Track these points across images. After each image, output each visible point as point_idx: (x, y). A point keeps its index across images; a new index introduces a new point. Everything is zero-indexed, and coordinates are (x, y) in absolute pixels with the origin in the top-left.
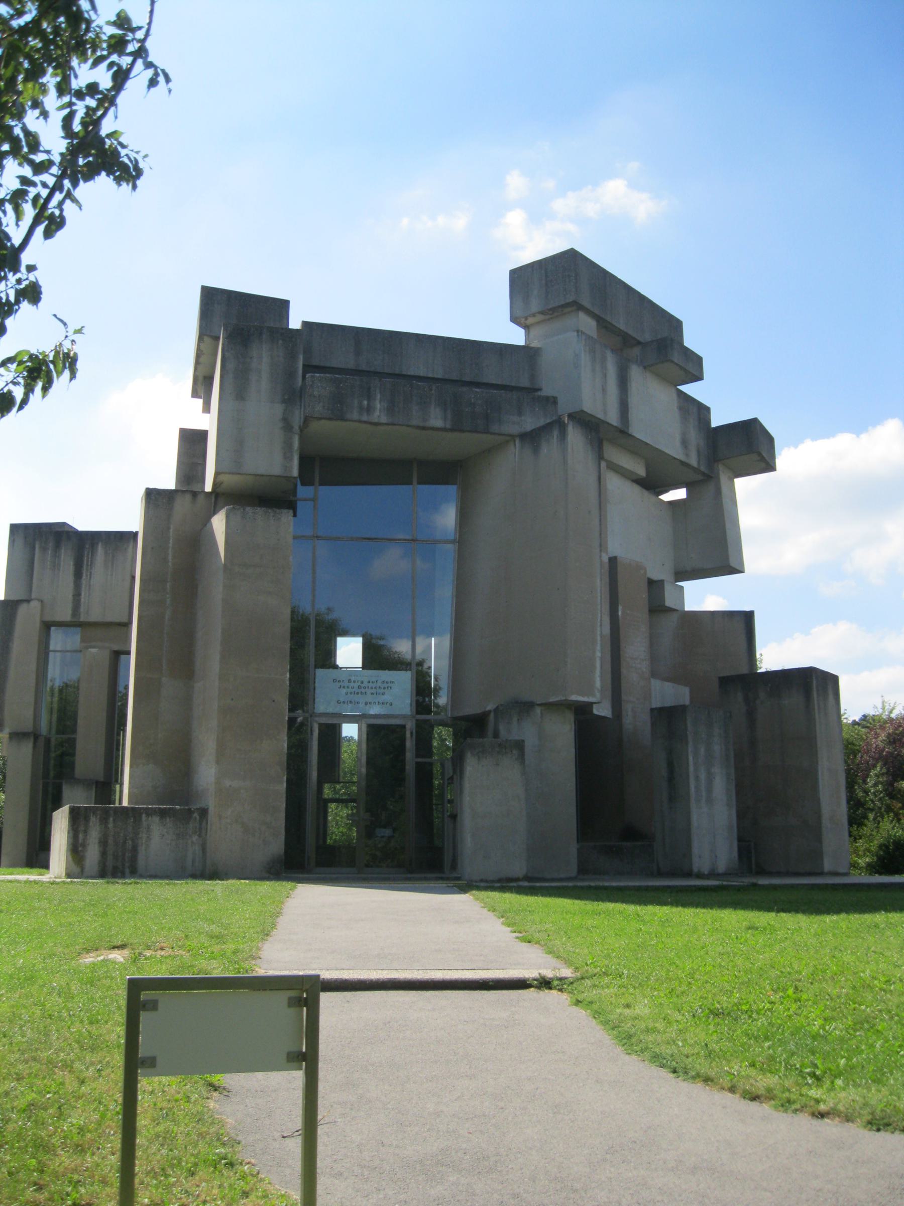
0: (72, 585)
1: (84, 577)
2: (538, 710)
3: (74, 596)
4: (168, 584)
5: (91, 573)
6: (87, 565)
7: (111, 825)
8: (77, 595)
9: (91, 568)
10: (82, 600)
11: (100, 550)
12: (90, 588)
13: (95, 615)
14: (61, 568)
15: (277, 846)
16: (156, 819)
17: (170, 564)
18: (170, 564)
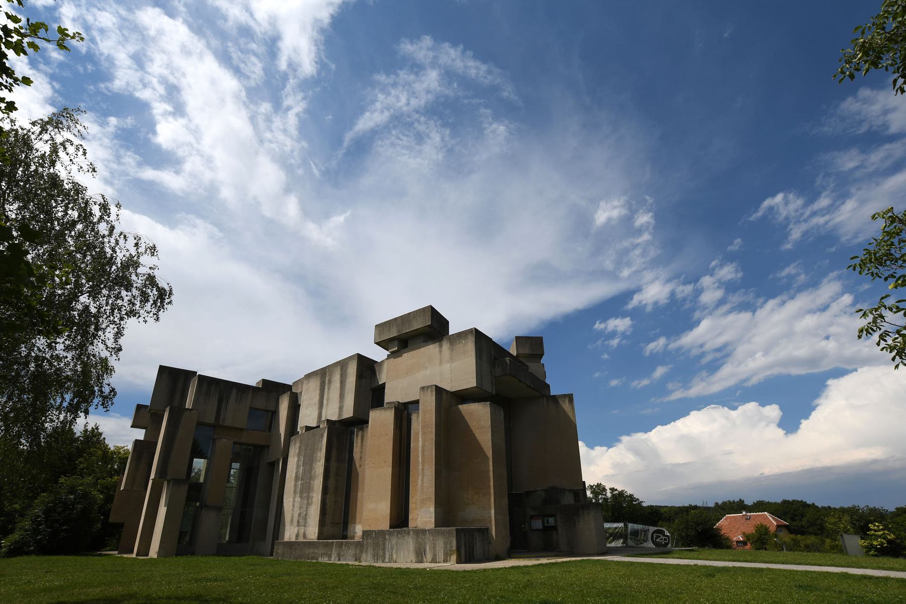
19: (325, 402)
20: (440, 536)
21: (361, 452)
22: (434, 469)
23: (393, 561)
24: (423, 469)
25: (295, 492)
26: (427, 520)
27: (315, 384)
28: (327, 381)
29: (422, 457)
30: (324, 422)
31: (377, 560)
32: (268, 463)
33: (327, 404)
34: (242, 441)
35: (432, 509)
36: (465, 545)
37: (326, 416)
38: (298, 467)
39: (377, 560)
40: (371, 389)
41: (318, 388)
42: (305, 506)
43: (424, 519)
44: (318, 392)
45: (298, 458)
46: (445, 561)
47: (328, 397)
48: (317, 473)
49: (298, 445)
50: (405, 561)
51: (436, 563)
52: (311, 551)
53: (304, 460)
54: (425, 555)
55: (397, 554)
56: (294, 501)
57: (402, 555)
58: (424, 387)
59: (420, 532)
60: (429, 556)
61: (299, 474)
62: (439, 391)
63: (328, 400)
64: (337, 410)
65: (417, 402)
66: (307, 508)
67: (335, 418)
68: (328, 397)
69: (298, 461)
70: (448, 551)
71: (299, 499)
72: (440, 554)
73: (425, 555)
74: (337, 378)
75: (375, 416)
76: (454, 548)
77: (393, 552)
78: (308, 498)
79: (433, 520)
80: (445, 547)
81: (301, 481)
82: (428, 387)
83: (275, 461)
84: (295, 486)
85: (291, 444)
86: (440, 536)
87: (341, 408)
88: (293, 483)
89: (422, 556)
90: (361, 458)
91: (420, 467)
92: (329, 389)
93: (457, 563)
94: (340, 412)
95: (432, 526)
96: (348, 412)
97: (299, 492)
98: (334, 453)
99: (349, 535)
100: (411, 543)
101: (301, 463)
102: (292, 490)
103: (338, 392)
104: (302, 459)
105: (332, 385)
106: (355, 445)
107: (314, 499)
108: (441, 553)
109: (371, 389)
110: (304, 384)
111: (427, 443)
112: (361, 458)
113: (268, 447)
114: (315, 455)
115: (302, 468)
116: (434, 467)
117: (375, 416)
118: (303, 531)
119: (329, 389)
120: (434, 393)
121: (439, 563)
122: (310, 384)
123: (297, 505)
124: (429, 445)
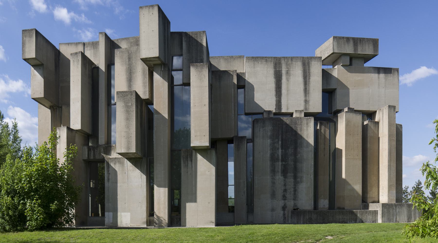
19: (284, 91)
26: (392, 198)
31: (390, 221)
33: (288, 94)
39: (390, 221)
52: (341, 217)
53: (282, 143)
55: (399, 218)
64: (303, 103)
71: (282, 178)
89: (410, 219)
97: (280, 171)
100: (405, 211)
103: (302, 87)
112: (324, 148)
119: (288, 80)
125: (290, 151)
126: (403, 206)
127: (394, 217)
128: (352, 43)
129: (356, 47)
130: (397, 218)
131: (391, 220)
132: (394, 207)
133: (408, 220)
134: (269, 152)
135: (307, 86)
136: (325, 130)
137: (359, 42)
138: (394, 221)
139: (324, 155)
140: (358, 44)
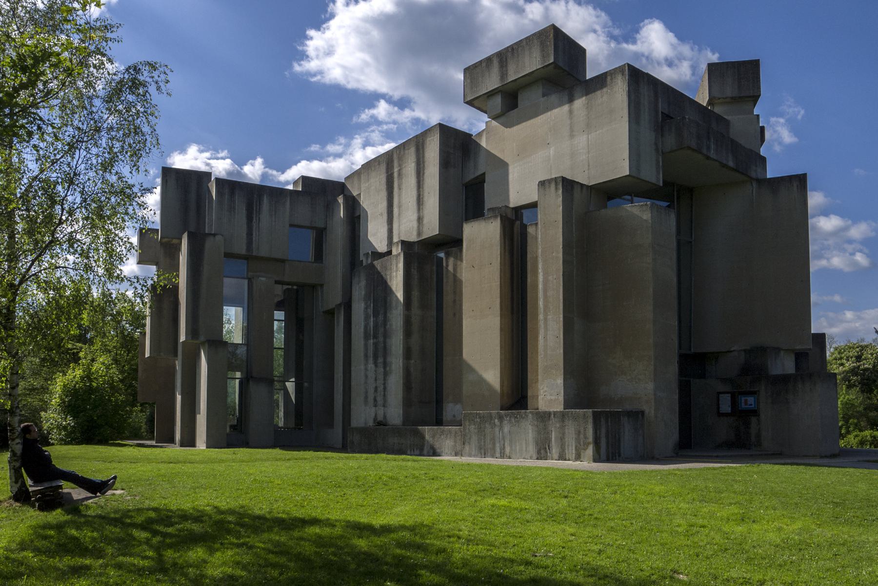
0: (245, 226)
1: (254, 220)
2: (782, 353)
3: (247, 234)
4: (574, 250)
5: (259, 218)
6: (256, 211)
7: (610, 424)
8: (250, 234)
9: (259, 214)
10: (254, 239)
11: (265, 200)
12: (259, 231)
13: (264, 252)
14: (236, 211)
15: (675, 436)
16: (626, 418)
17: (574, 235)
18: (574, 235)
20: (570, 422)
21: (455, 293)
22: (562, 319)
23: (506, 456)
24: (546, 319)
25: (366, 356)
26: (553, 398)
27: (378, 180)
28: (396, 175)
29: (544, 300)
30: (398, 246)
32: (323, 312)
33: (399, 214)
34: (286, 279)
35: (560, 381)
36: (607, 437)
37: (399, 234)
38: (367, 318)
40: (463, 185)
41: (384, 187)
42: (381, 377)
43: (549, 397)
44: (384, 194)
45: (366, 304)
46: (578, 458)
47: (399, 202)
48: (394, 327)
49: (363, 283)
50: (523, 456)
51: (565, 460)
53: (373, 306)
54: (549, 449)
56: (366, 369)
57: (518, 448)
58: (544, 181)
59: (544, 417)
60: (555, 451)
61: (369, 328)
62: (568, 185)
63: (400, 207)
64: (415, 224)
65: (534, 205)
66: (385, 379)
67: (413, 238)
68: (399, 202)
69: (366, 308)
70: (582, 443)
71: (373, 366)
72: (570, 448)
73: (549, 449)
74: (410, 167)
75: (472, 231)
76: (591, 439)
77: (506, 444)
78: (385, 364)
79: (561, 398)
80: (578, 440)
81: (373, 339)
82: (550, 181)
83: (334, 309)
84: (366, 345)
85: (353, 282)
86: (570, 422)
87: (420, 219)
88: (362, 342)
89: (546, 452)
90: (454, 301)
91: (541, 317)
92: (400, 189)
93: (595, 461)
94: (419, 227)
95: (560, 408)
96: (432, 227)
98: (415, 294)
99: (444, 419)
100: (530, 431)
101: (370, 311)
102: (362, 354)
103: (414, 193)
104: (372, 305)
105: (404, 180)
106: (445, 280)
107: (393, 367)
108: (572, 446)
109: (463, 185)
110: (362, 181)
111: (550, 278)
112: (454, 301)
113: (322, 286)
114: (389, 298)
115: (372, 319)
116: (562, 316)
117: (472, 231)
118: (383, 412)
119: (400, 189)
120: (560, 191)
121: (569, 460)
122: (372, 180)
123: (371, 374)
124: (555, 281)
125: (381, 318)
126: (524, 418)
127: (498, 445)
128: (497, 64)
129: (504, 69)
130: (504, 447)
131: (489, 450)
132: (496, 420)
133: (539, 452)
134: (363, 323)
135: (421, 189)
136: (456, 265)
137: (509, 55)
138: (498, 455)
139: (454, 314)
140: (509, 60)
